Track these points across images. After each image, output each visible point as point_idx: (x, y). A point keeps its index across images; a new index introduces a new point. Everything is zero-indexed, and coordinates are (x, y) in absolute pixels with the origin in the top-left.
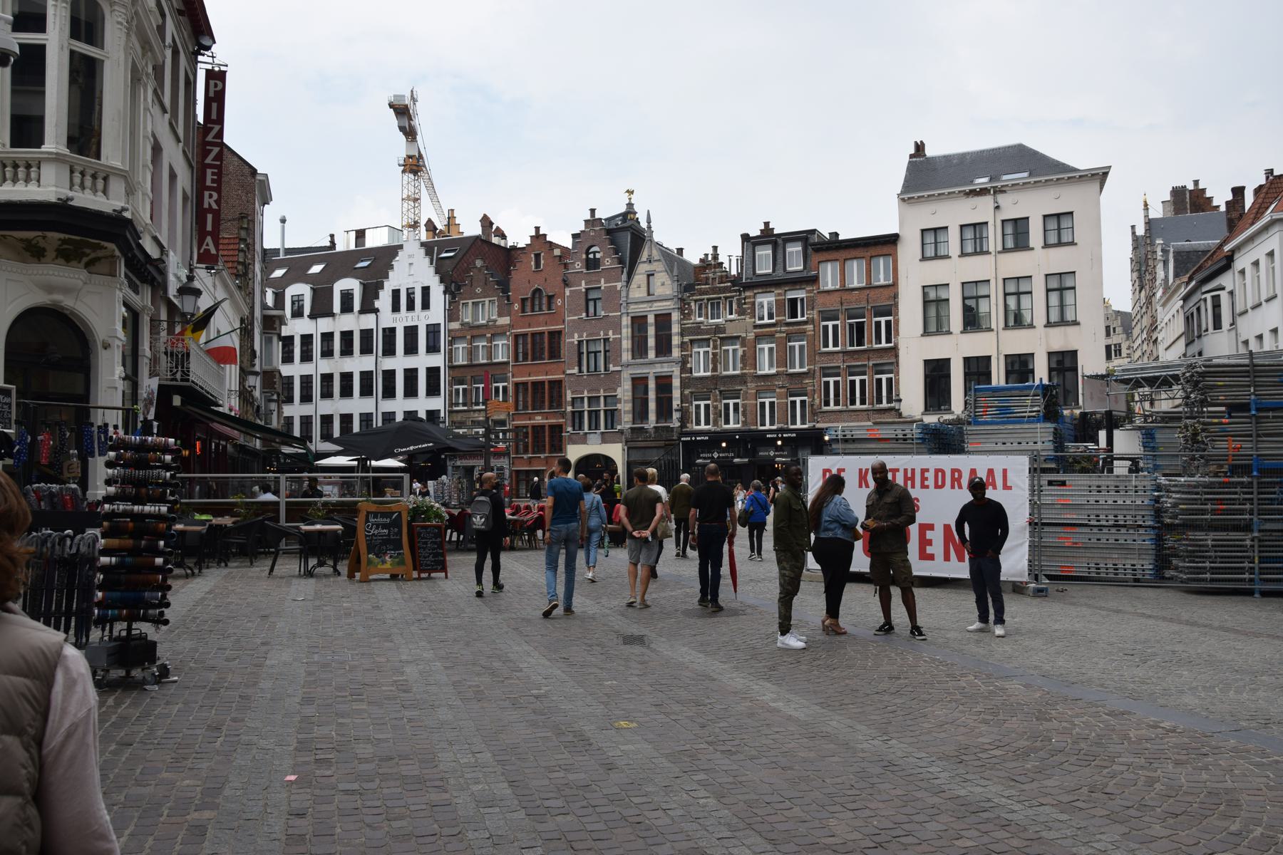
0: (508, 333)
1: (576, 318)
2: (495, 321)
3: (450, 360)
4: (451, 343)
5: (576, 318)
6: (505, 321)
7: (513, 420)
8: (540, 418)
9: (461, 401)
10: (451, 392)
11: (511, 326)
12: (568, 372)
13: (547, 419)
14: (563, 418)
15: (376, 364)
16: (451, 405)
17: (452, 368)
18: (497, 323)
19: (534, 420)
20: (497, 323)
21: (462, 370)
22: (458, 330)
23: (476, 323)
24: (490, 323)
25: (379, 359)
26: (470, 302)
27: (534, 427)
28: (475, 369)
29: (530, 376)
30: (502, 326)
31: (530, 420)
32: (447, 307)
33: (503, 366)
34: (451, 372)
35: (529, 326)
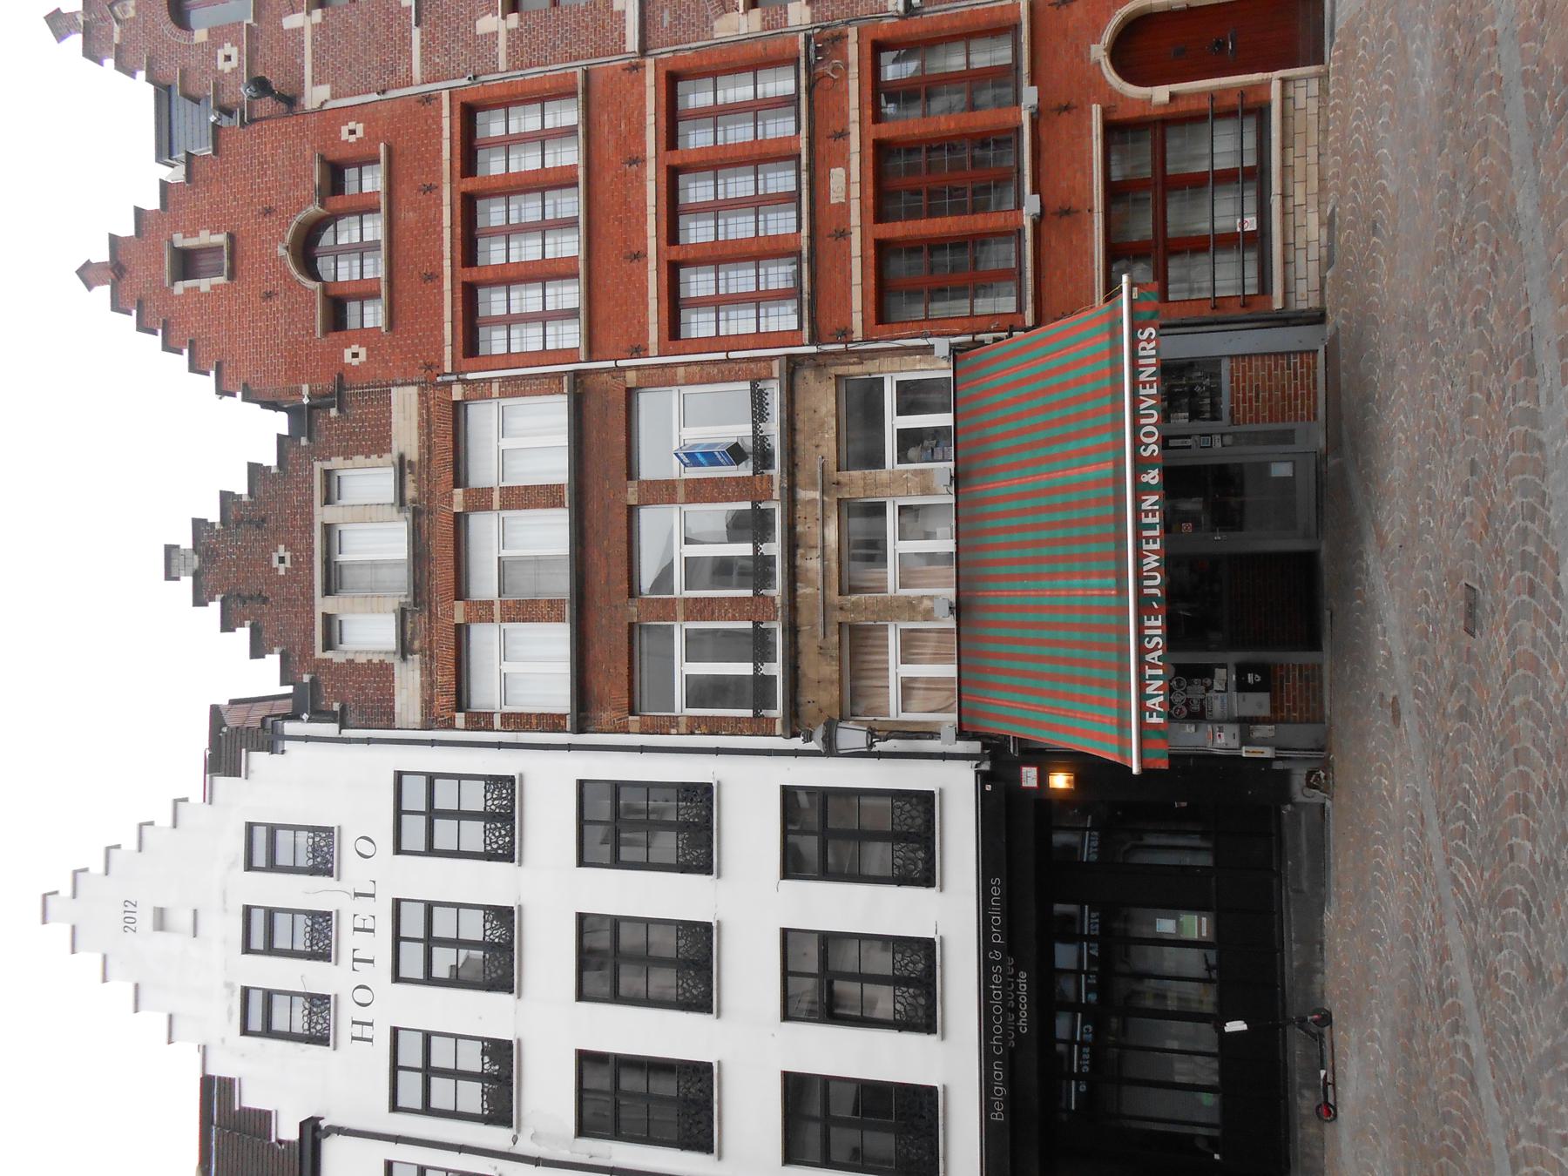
0: (457, 393)
1: (416, 34)
2: (402, 465)
3: (551, 722)
4: (480, 721)
5: (416, 34)
6: (405, 405)
7: (845, 334)
8: (837, 175)
9: (746, 669)
10: (695, 726)
11: (430, 382)
12: (632, 43)
13: (844, 134)
14: (842, 37)
15: (537, 1162)
16: (760, 726)
17: (584, 713)
18: (413, 454)
19: (844, 208)
20: (413, 454)
21: (596, 651)
22: (427, 671)
23: (401, 579)
24: (411, 493)
25: (525, 1147)
26: (323, 605)
27: (882, 205)
28: (598, 579)
29: (640, 256)
30: (426, 426)
31: (844, 234)
32: (331, 729)
33: (592, 405)
34: (606, 716)
35: (434, 277)
